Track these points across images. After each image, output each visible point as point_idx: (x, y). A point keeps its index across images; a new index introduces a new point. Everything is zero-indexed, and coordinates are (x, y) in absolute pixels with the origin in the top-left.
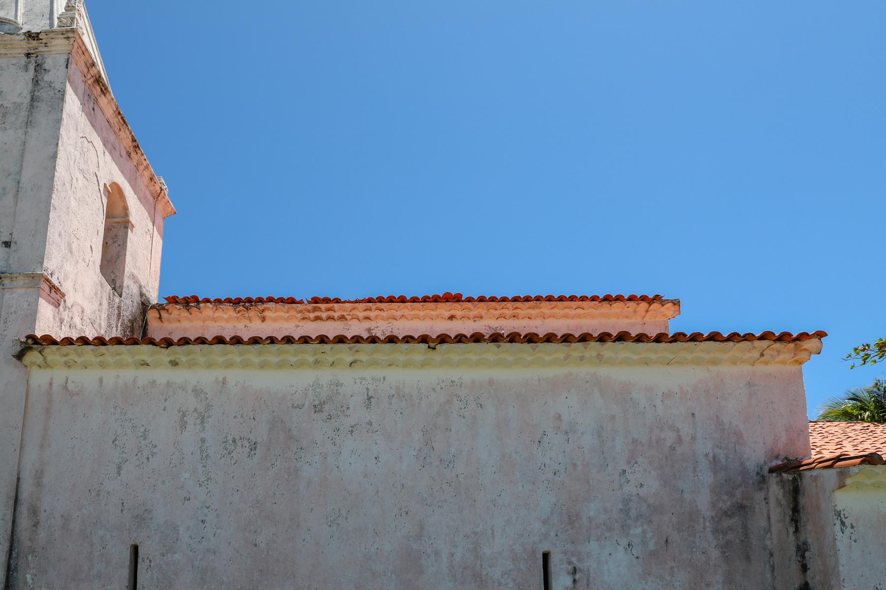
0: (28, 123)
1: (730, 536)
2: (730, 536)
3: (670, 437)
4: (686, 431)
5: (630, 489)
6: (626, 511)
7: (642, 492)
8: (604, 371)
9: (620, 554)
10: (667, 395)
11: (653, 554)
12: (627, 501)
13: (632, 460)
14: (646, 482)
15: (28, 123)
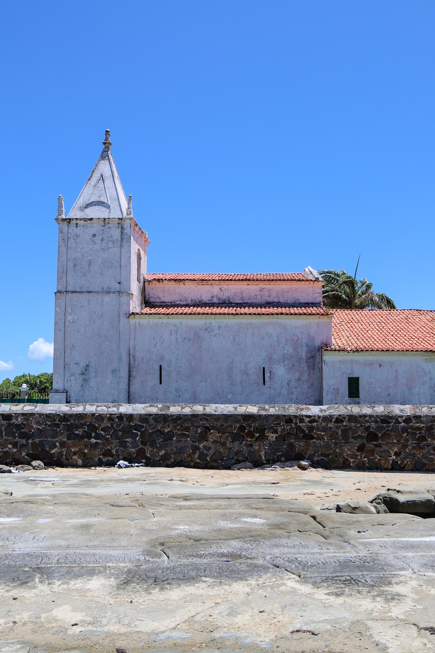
0: (121, 246)
1: (310, 364)
2: (310, 364)
3: (296, 338)
4: (300, 336)
5: (285, 351)
6: (284, 357)
7: (288, 352)
8: (279, 321)
9: (282, 368)
10: (296, 327)
11: (290, 368)
12: (284, 355)
13: (286, 344)
14: (289, 350)
15: (121, 246)
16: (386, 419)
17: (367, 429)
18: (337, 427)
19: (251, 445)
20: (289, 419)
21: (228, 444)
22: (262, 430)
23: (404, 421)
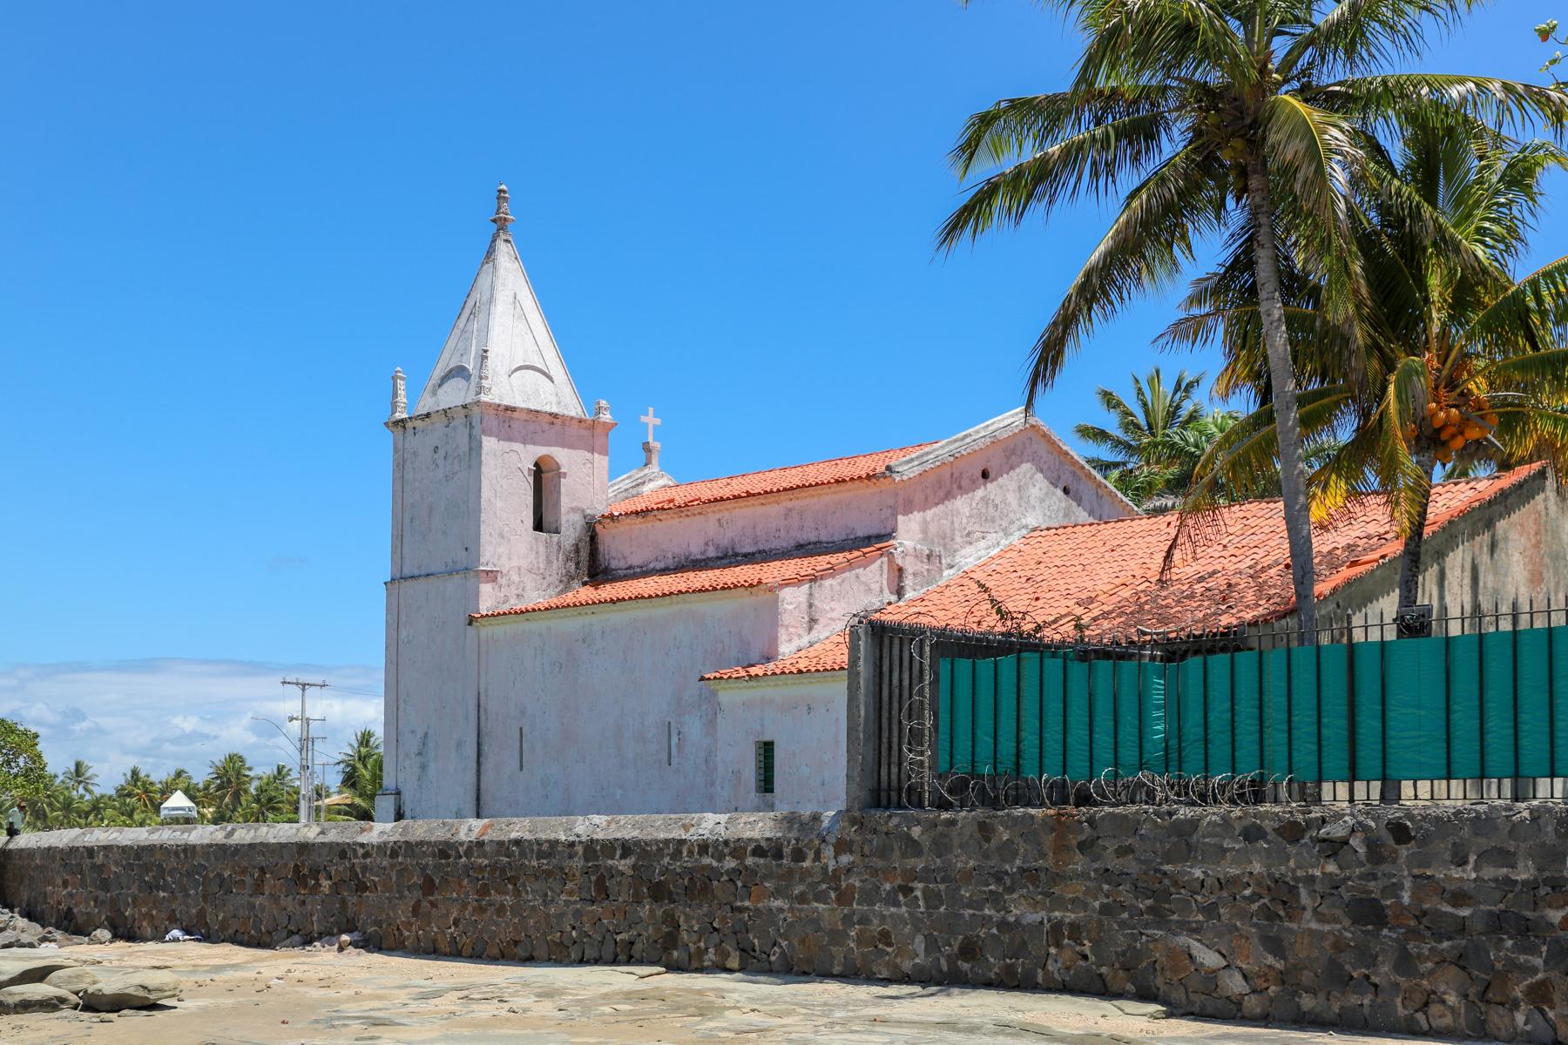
16: (445, 850)
17: (423, 869)
18: (392, 866)
19: (304, 903)
20: (342, 851)
21: (283, 902)
22: (315, 873)
23: (468, 853)
